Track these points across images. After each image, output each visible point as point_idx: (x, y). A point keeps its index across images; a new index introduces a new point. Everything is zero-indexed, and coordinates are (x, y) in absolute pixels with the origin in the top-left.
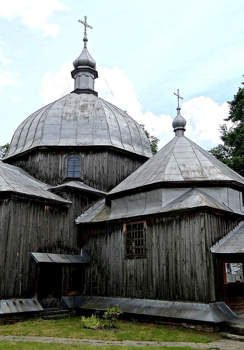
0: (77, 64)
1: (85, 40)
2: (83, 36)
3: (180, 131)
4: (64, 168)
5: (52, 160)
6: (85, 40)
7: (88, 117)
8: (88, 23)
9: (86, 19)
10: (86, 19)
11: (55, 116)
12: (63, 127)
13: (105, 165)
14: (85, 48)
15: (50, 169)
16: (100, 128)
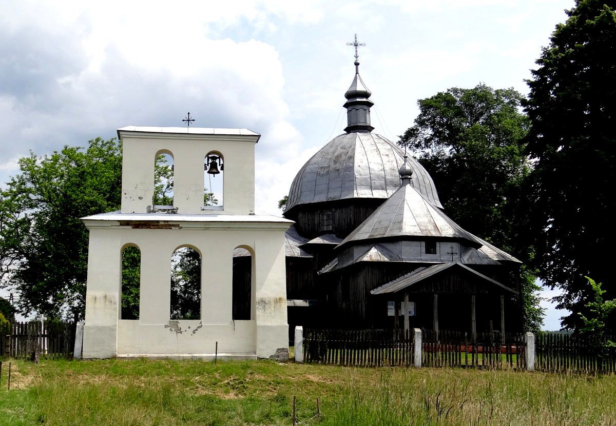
0: (349, 96)
1: (357, 64)
2: (354, 60)
3: (407, 181)
4: (319, 223)
5: (309, 216)
6: (357, 64)
7: (339, 170)
8: (359, 41)
9: (356, 38)
10: (356, 38)
11: (312, 172)
12: (317, 183)
13: (352, 216)
14: (357, 73)
15: (308, 225)
16: (348, 180)
